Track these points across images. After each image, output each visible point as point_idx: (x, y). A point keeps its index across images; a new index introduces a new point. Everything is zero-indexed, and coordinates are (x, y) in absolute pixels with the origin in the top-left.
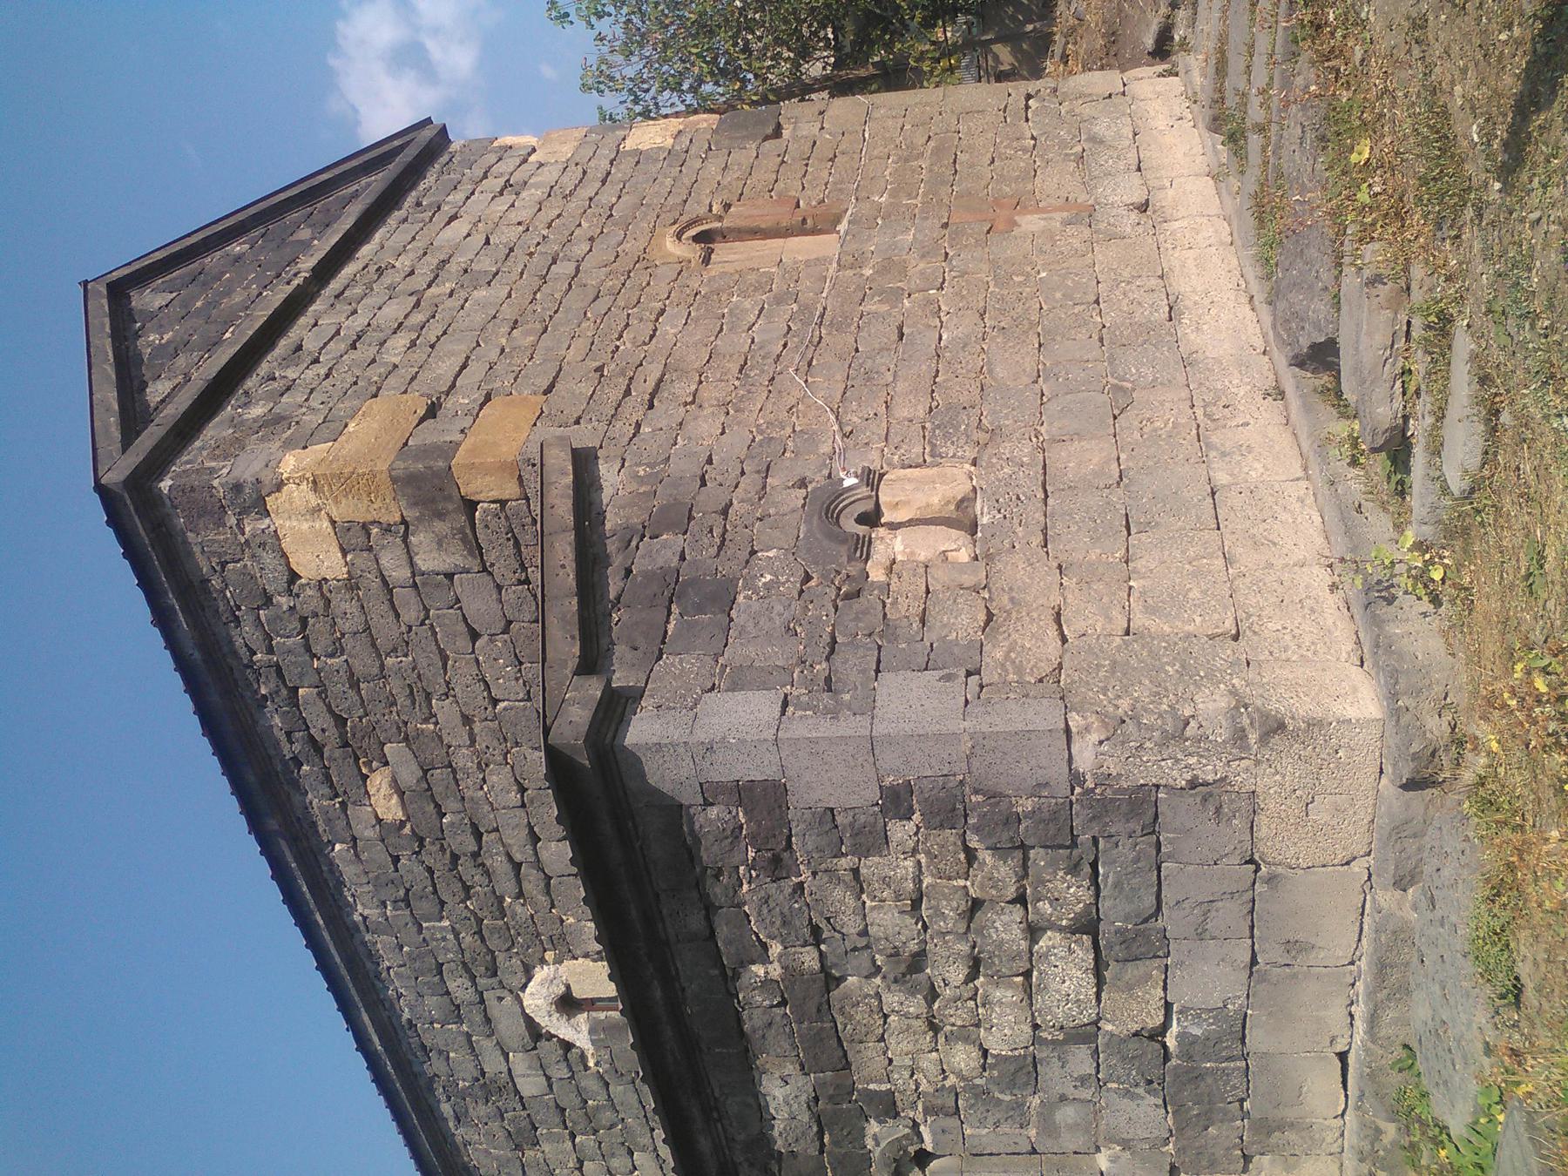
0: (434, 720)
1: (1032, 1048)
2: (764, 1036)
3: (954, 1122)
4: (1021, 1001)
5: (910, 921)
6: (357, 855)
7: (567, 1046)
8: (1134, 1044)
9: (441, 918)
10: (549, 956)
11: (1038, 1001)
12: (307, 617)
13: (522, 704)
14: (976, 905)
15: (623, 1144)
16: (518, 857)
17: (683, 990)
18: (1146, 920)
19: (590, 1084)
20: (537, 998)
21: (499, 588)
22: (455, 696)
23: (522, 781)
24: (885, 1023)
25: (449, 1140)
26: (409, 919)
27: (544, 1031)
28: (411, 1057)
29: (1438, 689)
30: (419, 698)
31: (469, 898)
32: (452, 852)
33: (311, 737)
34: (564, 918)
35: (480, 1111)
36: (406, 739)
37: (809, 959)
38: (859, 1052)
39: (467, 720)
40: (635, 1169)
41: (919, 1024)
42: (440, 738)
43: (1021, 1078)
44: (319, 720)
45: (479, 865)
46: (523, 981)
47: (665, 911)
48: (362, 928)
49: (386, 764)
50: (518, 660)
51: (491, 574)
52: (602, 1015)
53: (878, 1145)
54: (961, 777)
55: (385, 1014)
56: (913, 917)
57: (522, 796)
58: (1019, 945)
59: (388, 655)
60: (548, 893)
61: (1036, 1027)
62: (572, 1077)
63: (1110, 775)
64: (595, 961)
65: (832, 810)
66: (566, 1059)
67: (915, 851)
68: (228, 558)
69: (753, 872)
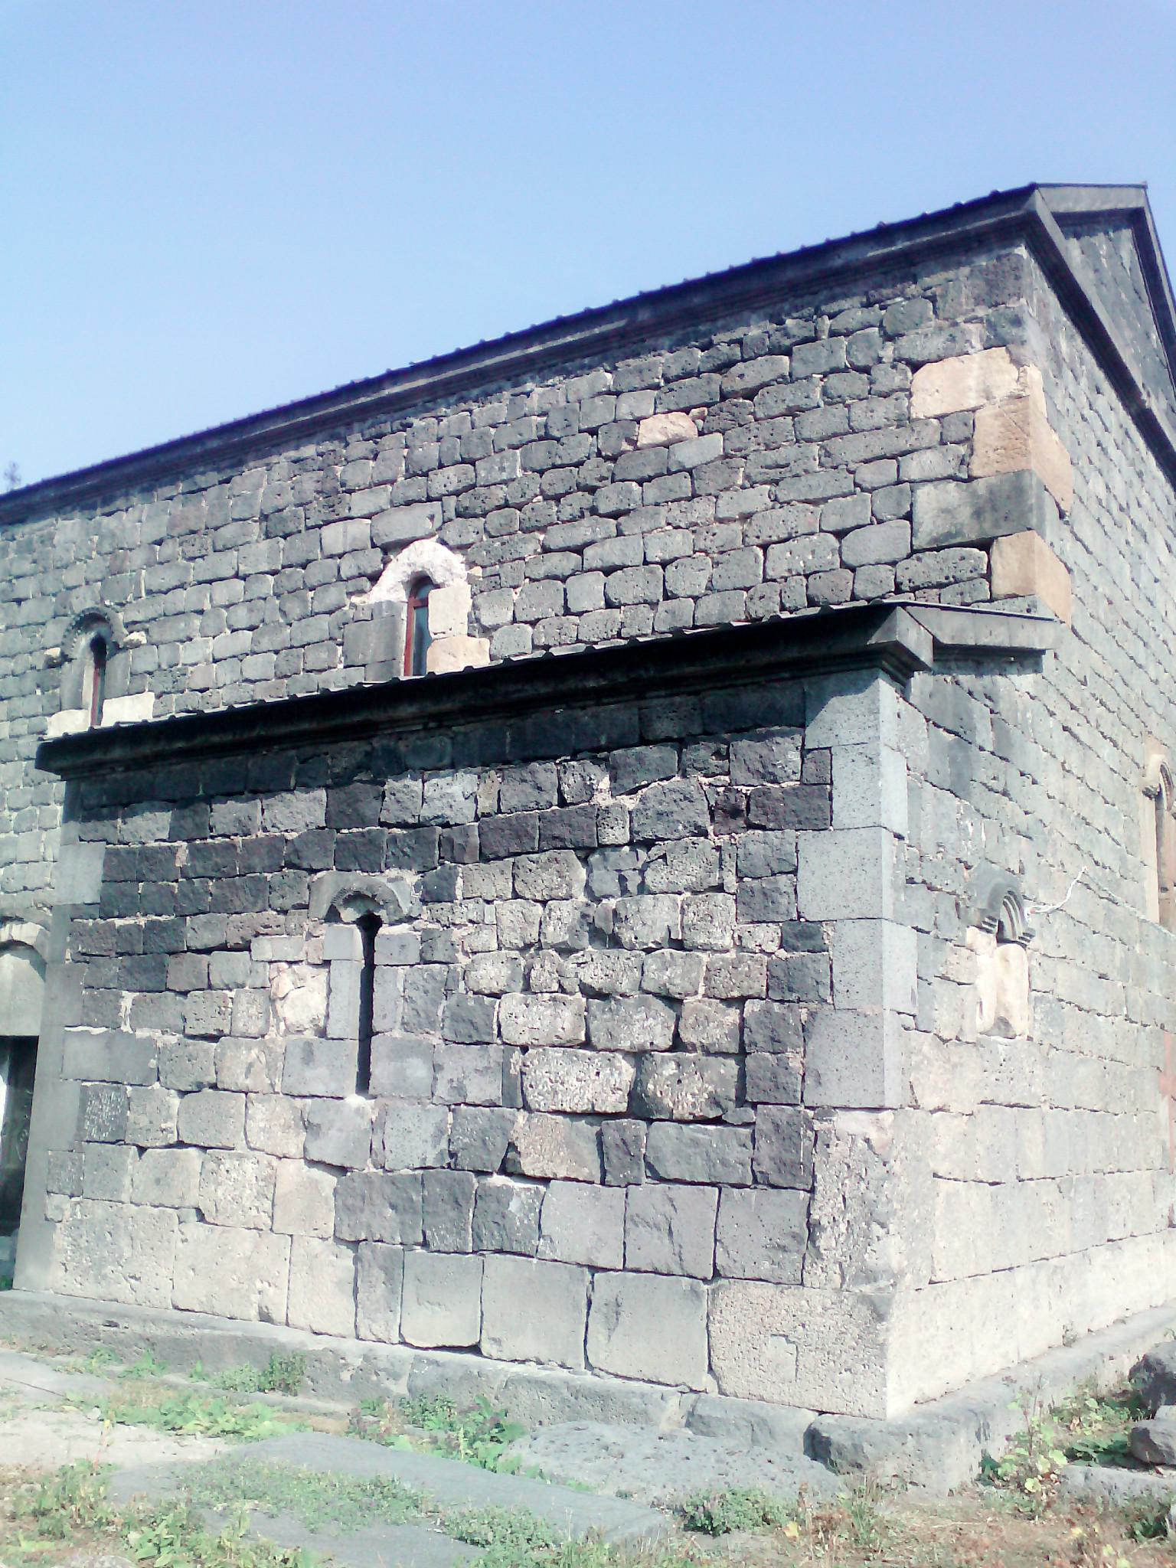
0: (748, 484)
1: (499, 1042)
2: (526, 781)
4: (557, 1037)
5: (660, 935)
6: (600, 394)
7: (374, 578)
8: (501, 1144)
9: (525, 470)
10: (477, 571)
11: (558, 1053)
12: (869, 373)
13: (761, 573)
14: (673, 1001)
15: (263, 621)
16: (588, 552)
17: (583, 708)
18: (649, 1166)
19: (333, 595)
20: (428, 555)
21: (894, 564)
22: (773, 508)
23: (674, 564)
24: (536, 901)
25: (273, 450)
26: (526, 437)
27: (392, 557)
28: (369, 422)
29: (921, 1478)
30: (774, 474)
31: (545, 499)
32: (599, 487)
33: (731, 364)
34: (518, 590)
35: (309, 483)
36: (726, 456)
37: (617, 834)
38: (502, 873)
39: (746, 517)
40: (233, 631)
41: (533, 935)
42: (727, 489)
43: (464, 1029)
44: (752, 373)
45: (582, 513)
46: (451, 543)
47: (677, 699)
48: (518, 390)
49: (701, 433)
50: (811, 574)
51: (909, 557)
52: (404, 616)
53: (391, 880)
54: (830, 1000)
55: (419, 402)
56: (663, 939)
57: (657, 563)
58: (625, 1039)
59: (822, 447)
60: (547, 577)
61: (524, 1049)
62: (340, 579)
63: (828, 1146)
64: (469, 615)
65: (795, 872)
66: (361, 575)
67: (741, 948)
68: (940, 303)
69: (723, 789)
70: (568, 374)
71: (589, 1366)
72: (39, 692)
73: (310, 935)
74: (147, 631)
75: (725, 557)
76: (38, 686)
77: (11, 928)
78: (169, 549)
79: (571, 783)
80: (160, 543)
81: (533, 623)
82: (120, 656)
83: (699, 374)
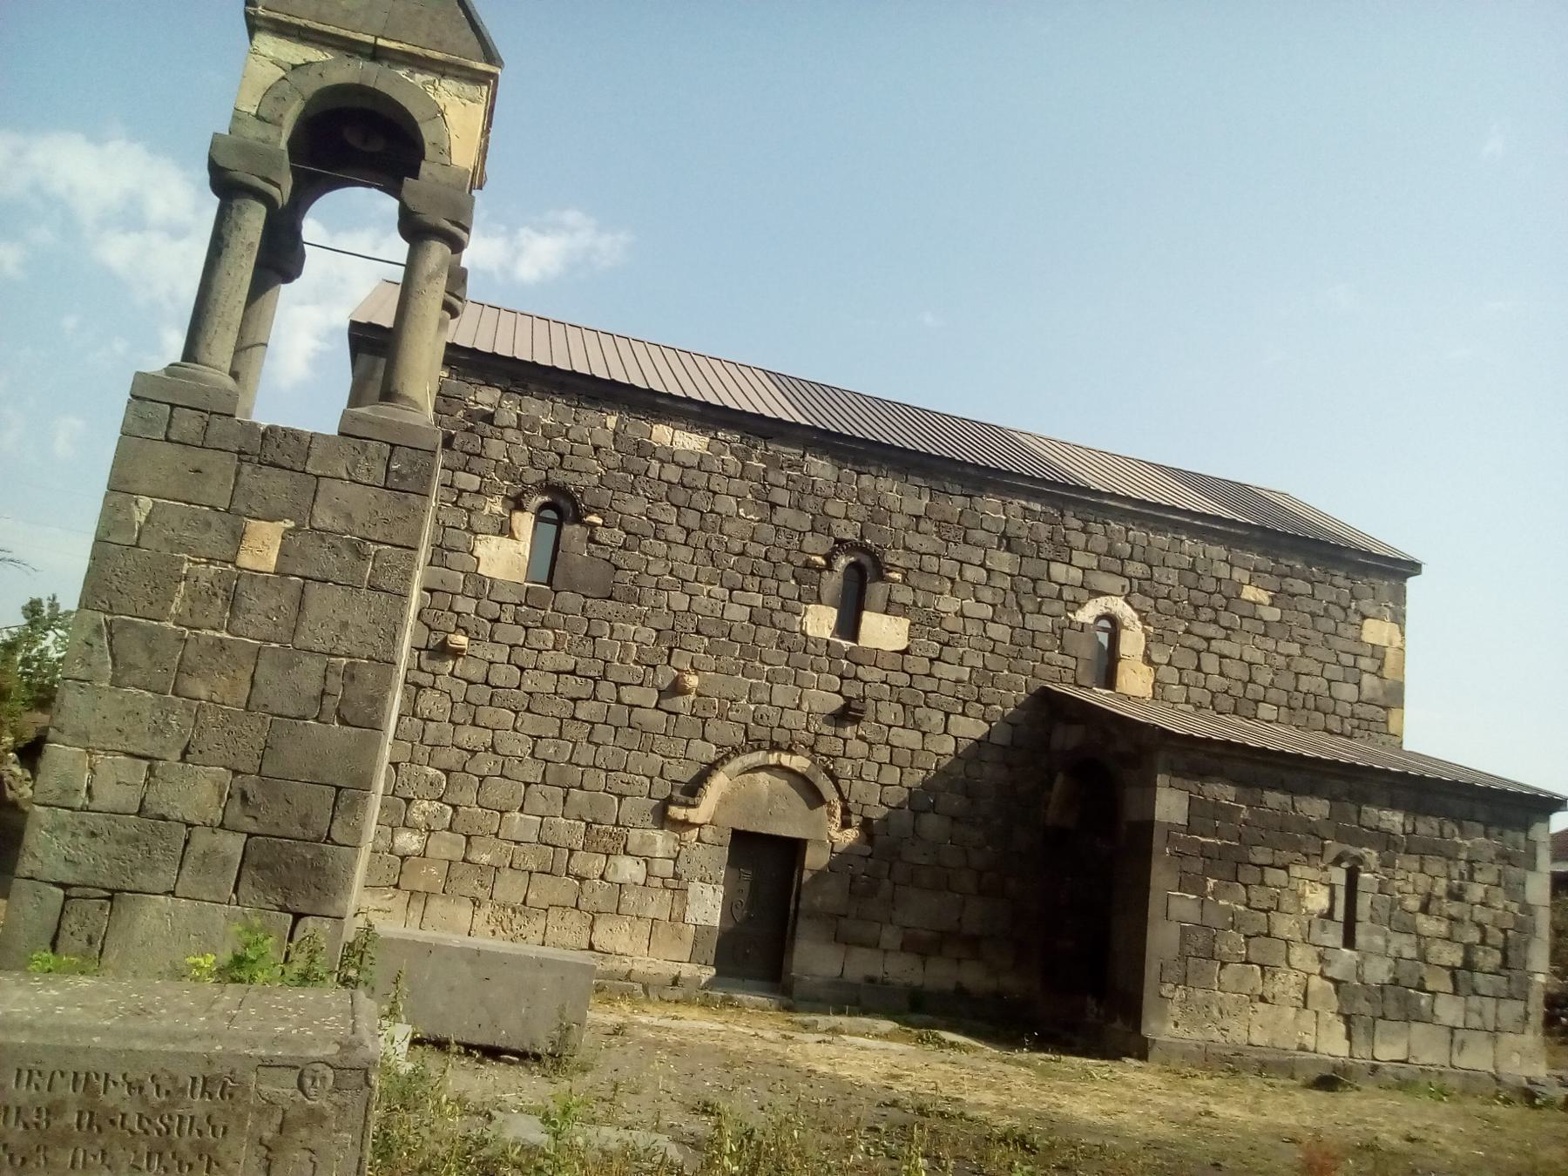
3: (1376, 890)
5: (1478, 900)
7: (1080, 605)
10: (1151, 629)
15: (1003, 604)
16: (1213, 642)
20: (1119, 606)
30: (1303, 640)
33: (1287, 576)
35: (1043, 530)
37: (1463, 855)
39: (1288, 656)
40: (977, 602)
48: (1176, 536)
49: (1272, 605)
65: (1524, 885)
70: (1205, 540)
71: (1452, 1066)
72: (793, 582)
73: (1325, 869)
74: (905, 576)
75: (1279, 672)
76: (794, 577)
77: (779, 756)
78: (923, 526)
79: (1447, 830)
80: (918, 517)
81: (1180, 669)
82: (880, 585)
83: (1270, 573)
